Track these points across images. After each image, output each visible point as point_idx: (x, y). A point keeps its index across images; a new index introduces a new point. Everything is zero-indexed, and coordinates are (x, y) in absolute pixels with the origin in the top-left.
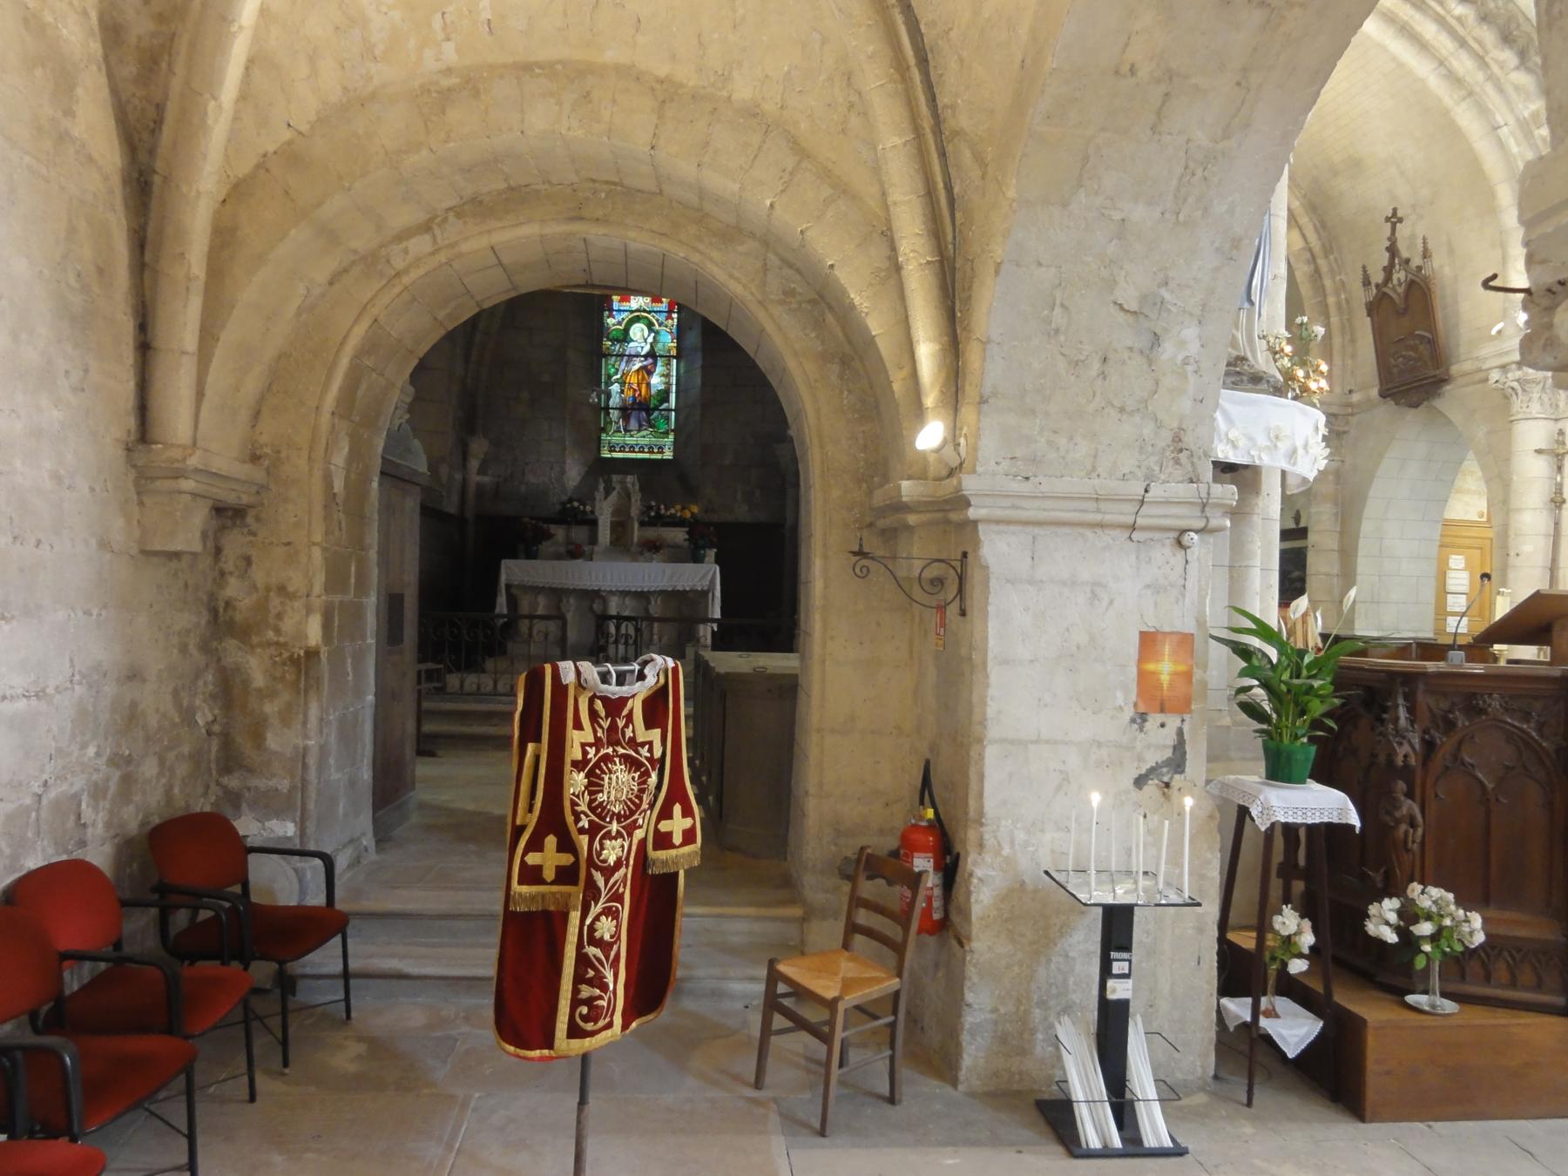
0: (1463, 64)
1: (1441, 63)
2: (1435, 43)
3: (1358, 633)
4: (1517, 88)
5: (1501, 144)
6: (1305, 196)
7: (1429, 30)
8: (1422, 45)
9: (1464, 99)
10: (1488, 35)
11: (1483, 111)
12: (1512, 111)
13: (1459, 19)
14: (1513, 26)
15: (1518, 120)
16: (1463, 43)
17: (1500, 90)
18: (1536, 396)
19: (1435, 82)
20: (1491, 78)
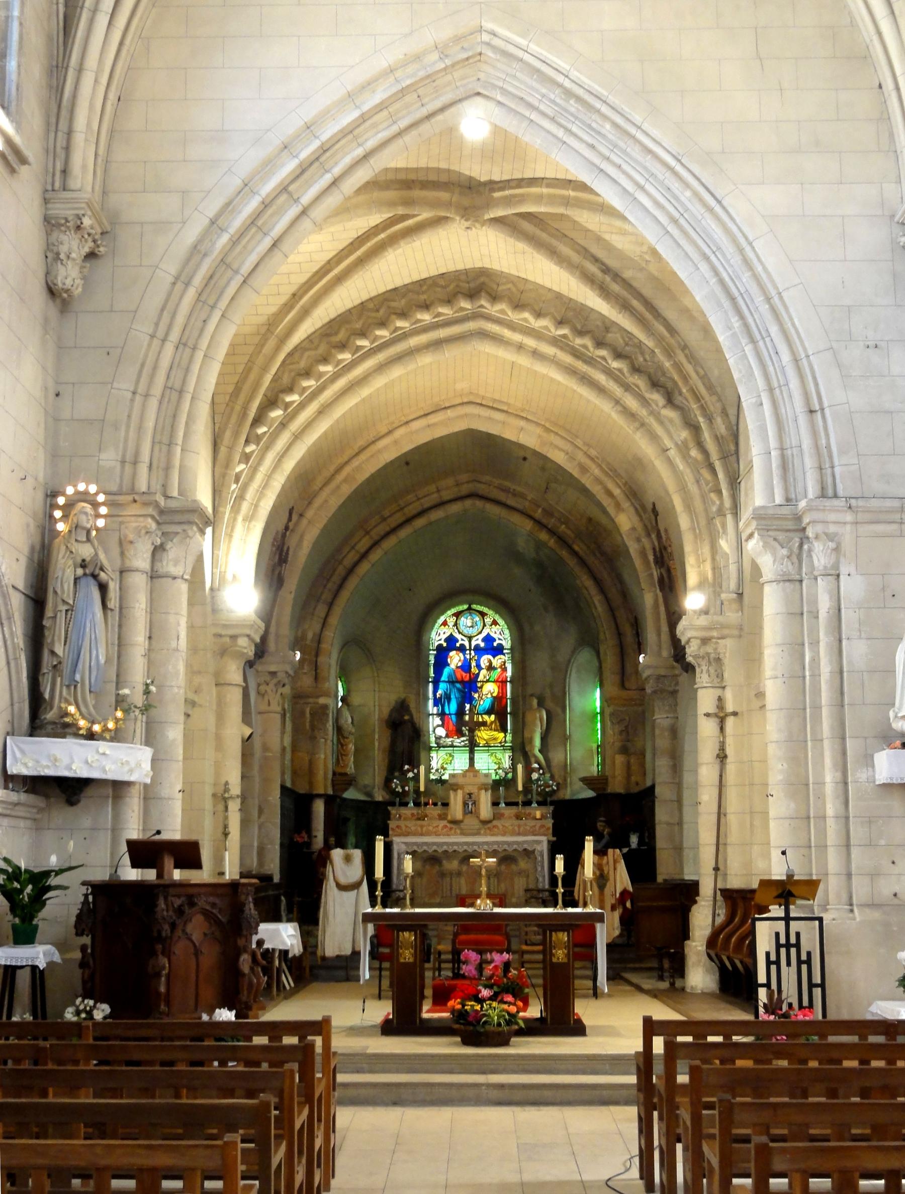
0: (631, 403)
1: (617, 402)
2: (607, 386)
3: (687, 878)
4: (671, 421)
5: (670, 462)
6: (626, 484)
7: (601, 378)
8: (601, 390)
9: (638, 429)
10: (640, 382)
11: (654, 437)
12: (671, 437)
13: (620, 370)
14: (660, 373)
15: (676, 444)
16: (627, 387)
17: (661, 423)
18: (704, 668)
19: (615, 416)
20: (652, 413)
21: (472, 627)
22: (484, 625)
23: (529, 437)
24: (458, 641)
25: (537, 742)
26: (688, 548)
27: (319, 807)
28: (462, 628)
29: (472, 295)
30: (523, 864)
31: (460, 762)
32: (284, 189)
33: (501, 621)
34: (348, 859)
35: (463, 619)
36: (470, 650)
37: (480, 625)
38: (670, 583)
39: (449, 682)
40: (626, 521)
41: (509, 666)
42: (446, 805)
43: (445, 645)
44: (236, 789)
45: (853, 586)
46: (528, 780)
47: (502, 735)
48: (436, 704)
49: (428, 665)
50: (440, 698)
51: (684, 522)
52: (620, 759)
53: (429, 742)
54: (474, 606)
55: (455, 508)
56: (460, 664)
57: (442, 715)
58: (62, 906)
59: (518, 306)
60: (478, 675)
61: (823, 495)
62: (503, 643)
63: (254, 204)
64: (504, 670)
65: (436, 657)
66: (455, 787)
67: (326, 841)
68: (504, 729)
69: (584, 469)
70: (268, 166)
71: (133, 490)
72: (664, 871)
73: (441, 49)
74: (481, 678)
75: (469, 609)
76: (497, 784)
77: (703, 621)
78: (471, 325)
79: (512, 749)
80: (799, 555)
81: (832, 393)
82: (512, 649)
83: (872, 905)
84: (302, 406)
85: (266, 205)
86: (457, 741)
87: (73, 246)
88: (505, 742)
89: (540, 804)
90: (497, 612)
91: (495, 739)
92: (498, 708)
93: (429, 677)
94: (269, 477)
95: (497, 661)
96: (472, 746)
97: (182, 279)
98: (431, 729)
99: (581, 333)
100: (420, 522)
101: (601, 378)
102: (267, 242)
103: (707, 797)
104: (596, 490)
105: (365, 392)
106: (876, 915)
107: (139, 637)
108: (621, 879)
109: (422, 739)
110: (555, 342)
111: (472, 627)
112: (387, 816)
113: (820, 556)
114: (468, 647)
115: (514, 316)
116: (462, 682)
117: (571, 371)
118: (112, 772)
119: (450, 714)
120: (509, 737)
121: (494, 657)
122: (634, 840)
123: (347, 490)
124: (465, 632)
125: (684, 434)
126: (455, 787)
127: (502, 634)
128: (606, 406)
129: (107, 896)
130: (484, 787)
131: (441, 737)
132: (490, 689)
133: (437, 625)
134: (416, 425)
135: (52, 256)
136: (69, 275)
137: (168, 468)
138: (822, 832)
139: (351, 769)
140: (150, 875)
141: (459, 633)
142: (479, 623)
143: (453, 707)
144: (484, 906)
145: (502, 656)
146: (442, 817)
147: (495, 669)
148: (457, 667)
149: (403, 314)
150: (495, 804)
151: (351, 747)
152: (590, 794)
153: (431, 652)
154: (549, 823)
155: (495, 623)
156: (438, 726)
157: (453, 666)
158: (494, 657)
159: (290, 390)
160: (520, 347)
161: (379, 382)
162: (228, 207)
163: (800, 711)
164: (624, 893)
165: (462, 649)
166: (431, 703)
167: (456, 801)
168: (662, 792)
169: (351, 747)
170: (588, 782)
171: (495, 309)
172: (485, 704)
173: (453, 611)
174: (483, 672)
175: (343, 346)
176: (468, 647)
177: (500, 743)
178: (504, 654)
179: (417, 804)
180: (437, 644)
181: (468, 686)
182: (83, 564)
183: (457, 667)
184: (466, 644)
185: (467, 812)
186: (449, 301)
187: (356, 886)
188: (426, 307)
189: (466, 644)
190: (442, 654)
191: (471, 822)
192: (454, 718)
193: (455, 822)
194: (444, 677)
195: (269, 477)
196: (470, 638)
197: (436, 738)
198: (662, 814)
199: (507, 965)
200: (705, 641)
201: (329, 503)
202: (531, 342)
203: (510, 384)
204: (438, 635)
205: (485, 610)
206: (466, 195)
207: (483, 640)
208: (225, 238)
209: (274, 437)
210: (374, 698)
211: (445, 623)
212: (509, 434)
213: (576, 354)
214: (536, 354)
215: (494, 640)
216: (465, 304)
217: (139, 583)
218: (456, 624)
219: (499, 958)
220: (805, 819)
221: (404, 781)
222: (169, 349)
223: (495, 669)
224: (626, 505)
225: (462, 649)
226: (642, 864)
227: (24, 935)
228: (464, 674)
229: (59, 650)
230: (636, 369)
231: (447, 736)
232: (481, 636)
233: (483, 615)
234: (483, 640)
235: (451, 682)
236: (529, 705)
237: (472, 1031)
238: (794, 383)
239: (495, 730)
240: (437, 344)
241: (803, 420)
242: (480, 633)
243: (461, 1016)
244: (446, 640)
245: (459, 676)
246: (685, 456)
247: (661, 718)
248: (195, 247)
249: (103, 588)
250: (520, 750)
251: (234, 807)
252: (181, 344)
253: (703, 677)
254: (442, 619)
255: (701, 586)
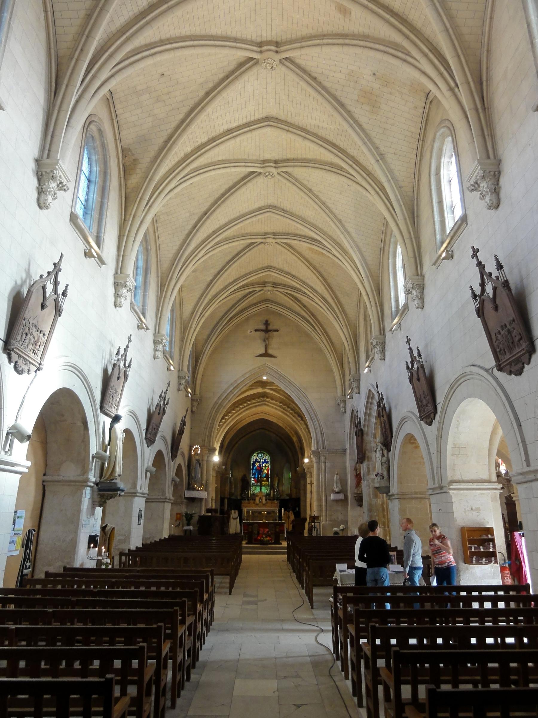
7: (289, 414)
11: (299, 426)
16: (294, 416)
23: (274, 420)
25: (276, 485)
26: (305, 449)
27: (226, 501)
29: (263, 397)
30: (272, 514)
31: (258, 490)
32: (231, 391)
34: (235, 513)
38: (303, 456)
40: (295, 439)
42: (255, 500)
44: (214, 498)
45: (328, 464)
46: (274, 495)
51: (305, 444)
52: (294, 490)
55: (258, 431)
57: (254, 478)
58: (196, 519)
59: (272, 399)
61: (323, 449)
63: (226, 394)
66: (257, 496)
67: (228, 508)
69: (286, 428)
70: (228, 388)
71: (204, 446)
72: (302, 516)
73: (259, 368)
76: (267, 495)
77: (308, 465)
78: (263, 403)
80: (319, 459)
81: (325, 431)
83: (330, 521)
84: (229, 419)
85: (228, 394)
86: (257, 484)
87: (195, 404)
89: (277, 500)
92: (267, 476)
94: (222, 433)
95: (267, 465)
96: (261, 486)
97: (213, 408)
99: (284, 405)
100: (250, 435)
101: (289, 414)
102: (228, 401)
103: (308, 500)
104: (289, 432)
105: (241, 416)
106: (331, 523)
107: (205, 472)
108: (292, 517)
110: (280, 406)
112: (241, 503)
113: (322, 459)
115: (271, 401)
117: (283, 412)
118: (202, 497)
122: (297, 509)
123: (235, 431)
125: (305, 426)
126: (257, 496)
127: (268, 459)
128: (289, 419)
129: (202, 519)
130: (264, 496)
132: (265, 471)
134: (250, 417)
135: (192, 406)
136: (195, 409)
137: (210, 442)
138: (322, 508)
139: (233, 492)
140: (210, 514)
143: (256, 476)
144: (264, 521)
146: (254, 503)
149: (249, 401)
150: (266, 500)
151: (233, 486)
152: (288, 498)
154: (279, 505)
159: (226, 416)
160: (273, 407)
161: (244, 414)
162: (221, 395)
163: (319, 486)
164: (293, 521)
165: (259, 462)
167: (257, 499)
168: (302, 498)
169: (233, 486)
170: (287, 495)
171: (268, 400)
172: (264, 475)
175: (237, 407)
179: (248, 500)
181: (260, 470)
182: (197, 460)
185: (260, 502)
186: (258, 398)
187: (236, 518)
188: (254, 399)
190: (254, 463)
191: (261, 504)
193: (257, 504)
195: (222, 433)
198: (302, 503)
199: (268, 532)
200: (308, 468)
201: (232, 433)
202: (275, 406)
203: (271, 412)
204: (253, 459)
206: (263, 384)
208: (221, 401)
209: (223, 425)
210: (239, 474)
212: (270, 420)
213: (284, 409)
214: (275, 409)
216: (262, 399)
217: (205, 462)
219: (267, 530)
220: (319, 506)
221: (245, 494)
222: (211, 420)
224: (295, 436)
225: (259, 462)
226: (297, 514)
227: (188, 525)
229: (193, 475)
230: (295, 413)
233: (264, 454)
235: (256, 470)
236: (275, 475)
237: (262, 543)
238: (319, 428)
240: (256, 406)
241: (320, 435)
243: (260, 540)
246: (305, 430)
247: (302, 482)
248: (215, 402)
249: (200, 464)
250: (272, 487)
251: (214, 502)
252: (213, 419)
253: (308, 476)
255: (308, 457)
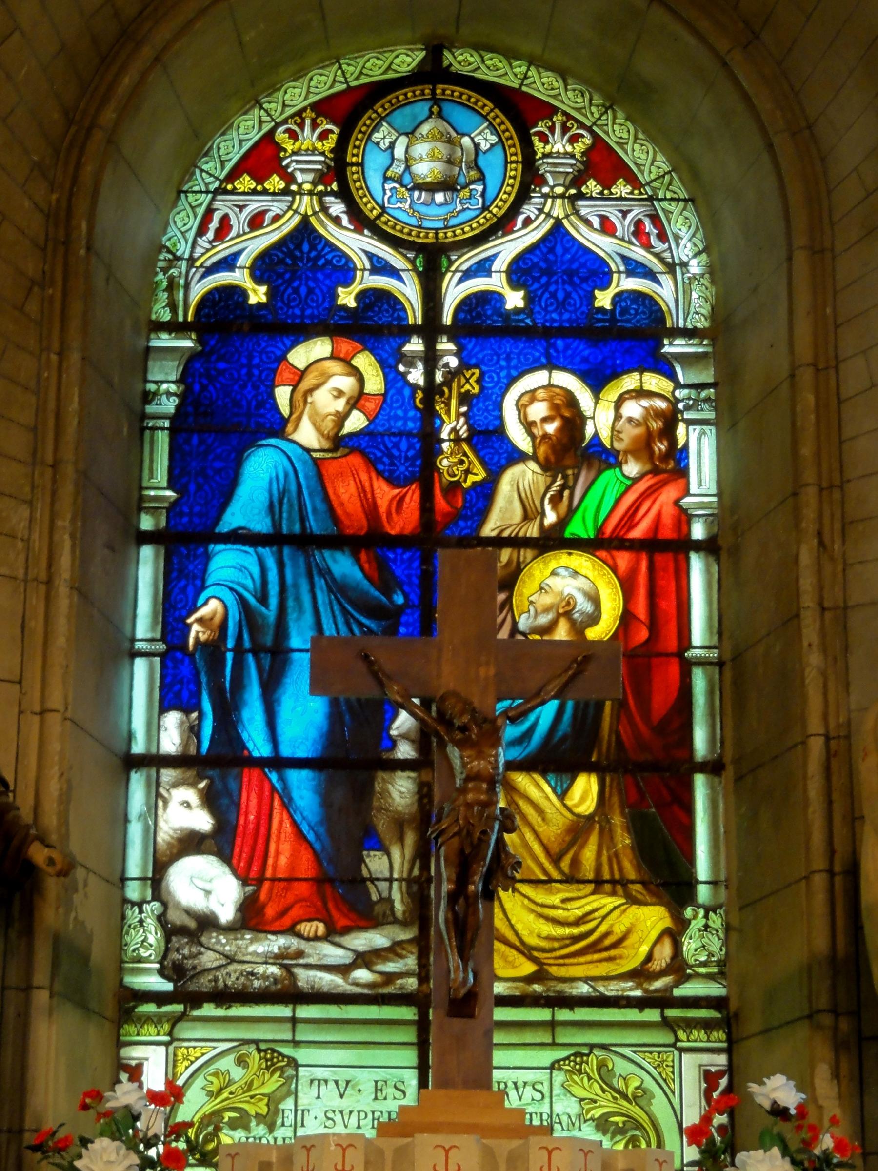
21: (447, 185)
22: (531, 178)
24: (344, 272)
28: (374, 184)
33: (642, 156)
35: (383, 135)
36: (431, 329)
37: (500, 174)
39: (273, 539)
41: (702, 449)
43: (258, 295)
47: (652, 919)
48: (173, 695)
49: (141, 427)
50: (213, 650)
53: (120, 961)
54: (461, 60)
56: (356, 422)
57: (218, 765)
60: (485, 493)
62: (665, 291)
64: (671, 465)
65: (192, 371)
68: (669, 881)
74: (503, 515)
75: (432, 74)
79: (726, 1017)
82: (721, 330)
86: (324, 958)
88: (679, 968)
90: (625, 92)
91: (603, 946)
93: (140, 505)
98: (136, 863)
109: (49, 916)
111: (447, 185)
114: (415, 314)
116: (369, 541)
119: (279, 763)
120: (701, 943)
121: (597, 382)
124: (402, 210)
131: (206, 922)
133: (211, 171)
141: (361, 221)
142: (492, 164)
143: (302, 718)
145: (654, 381)
147: (601, 457)
148: (339, 442)
153: (164, 340)
155: (602, 165)
156: (190, 843)
157: (307, 434)
158: (597, 382)
166: (142, 676)
173: (323, 83)
174: (521, 478)
176: (415, 314)
177: (640, 974)
178: (664, 367)
180: (199, 290)
183: (339, 442)
184: (409, 291)
189: (409, 291)
192: (302, 786)
194: (247, 508)
196: (432, 260)
197: (170, 931)
205: (542, 84)
207: (519, 272)
211: (263, 160)
215: (600, 274)
218: (338, 174)
223: (601, 457)
225: (373, 325)
228: (384, 493)
231: (251, 917)
232: (507, 249)
233: (521, 114)
234: (518, 273)
239: (598, 884)
242: (503, 225)
244: (263, 267)
245: (346, 493)
254: (246, 131)
